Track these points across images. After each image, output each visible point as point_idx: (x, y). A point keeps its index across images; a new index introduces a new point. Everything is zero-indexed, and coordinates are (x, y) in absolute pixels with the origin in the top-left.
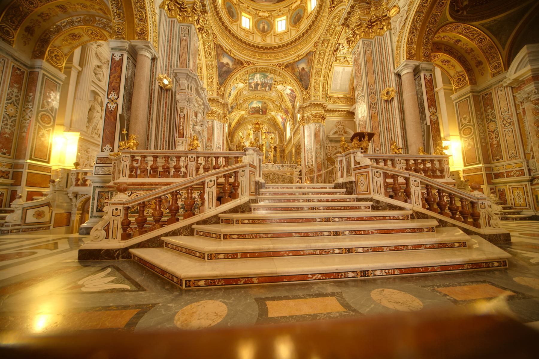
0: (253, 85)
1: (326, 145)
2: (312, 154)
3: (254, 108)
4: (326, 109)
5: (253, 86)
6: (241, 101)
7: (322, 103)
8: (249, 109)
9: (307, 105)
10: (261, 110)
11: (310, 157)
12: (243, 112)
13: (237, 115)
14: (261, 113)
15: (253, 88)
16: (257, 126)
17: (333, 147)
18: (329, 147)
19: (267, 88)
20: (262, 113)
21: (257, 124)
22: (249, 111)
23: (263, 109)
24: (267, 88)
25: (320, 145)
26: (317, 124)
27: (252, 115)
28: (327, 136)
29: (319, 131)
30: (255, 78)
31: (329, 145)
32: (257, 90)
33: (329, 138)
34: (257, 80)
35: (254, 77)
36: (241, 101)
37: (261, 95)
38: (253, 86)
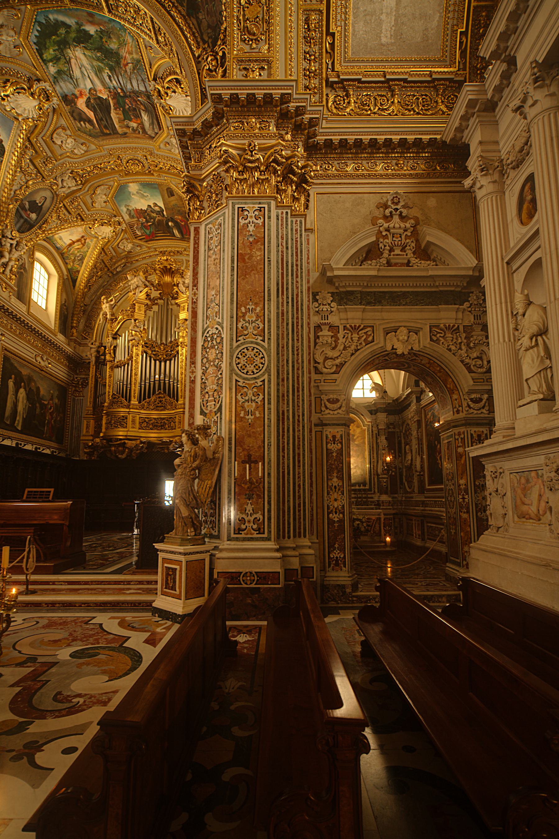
0: (81, 103)
1: (316, 319)
2: (219, 368)
3: (141, 213)
4: (320, 139)
5: (91, 114)
6: (71, 184)
7: (277, 93)
8: (127, 217)
9: (209, 116)
10: (172, 220)
11: (211, 386)
12: (107, 231)
13: (91, 243)
14: (176, 232)
15: (90, 121)
16: (167, 279)
17: (355, 329)
18: (332, 327)
19: (145, 117)
20: (180, 232)
21: (167, 271)
22: (131, 226)
23: (178, 218)
24: (145, 117)
25: (261, 317)
26: (251, 207)
27: (152, 244)
28: (323, 273)
29: (260, 240)
30: (77, 73)
31: (334, 319)
32: (114, 132)
33: (330, 281)
34: (89, 85)
35: (69, 62)
36: (71, 184)
37: (139, 156)
38: (91, 114)
